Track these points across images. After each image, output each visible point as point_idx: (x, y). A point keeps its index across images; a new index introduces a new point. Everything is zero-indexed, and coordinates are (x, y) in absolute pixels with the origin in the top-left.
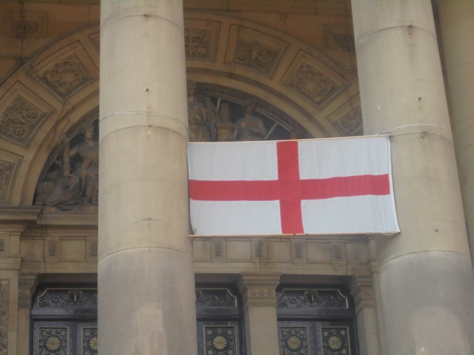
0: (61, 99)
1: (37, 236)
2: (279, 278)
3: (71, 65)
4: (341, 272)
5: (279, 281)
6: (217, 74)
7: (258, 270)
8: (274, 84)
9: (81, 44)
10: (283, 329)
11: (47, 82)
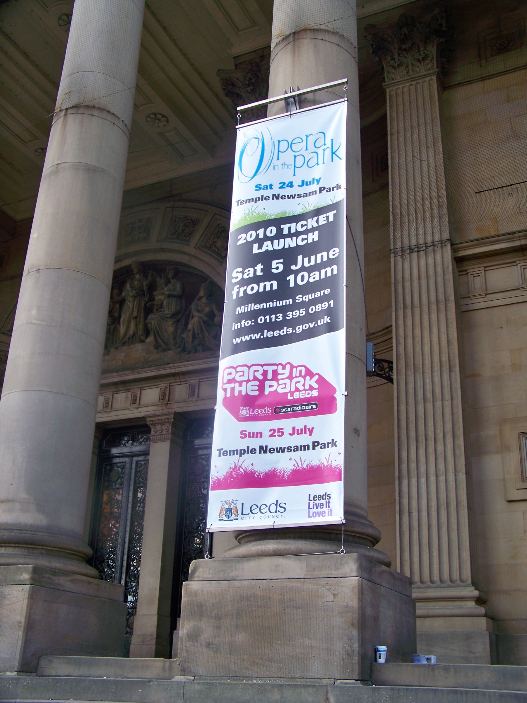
2: (172, 416)
7: (161, 411)
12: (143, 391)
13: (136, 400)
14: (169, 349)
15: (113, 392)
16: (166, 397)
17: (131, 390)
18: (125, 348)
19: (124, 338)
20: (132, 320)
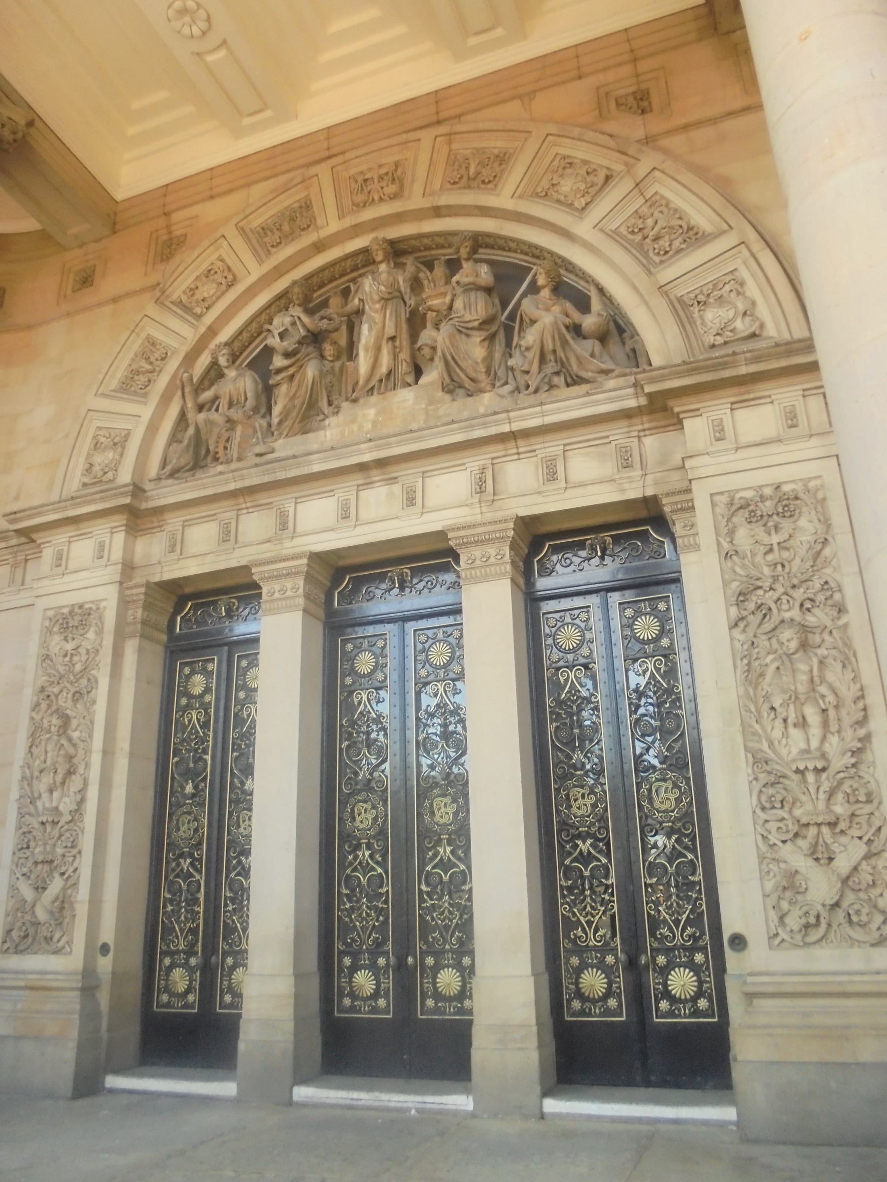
1: (154, 528)
2: (512, 525)
4: (633, 493)
5: (514, 529)
7: (479, 516)
8: (502, 199)
10: (549, 616)
12: (427, 480)
13: (414, 499)
14: (482, 391)
15: (358, 486)
16: (485, 488)
17: (399, 479)
18: (374, 399)
19: (368, 380)
20: (384, 342)
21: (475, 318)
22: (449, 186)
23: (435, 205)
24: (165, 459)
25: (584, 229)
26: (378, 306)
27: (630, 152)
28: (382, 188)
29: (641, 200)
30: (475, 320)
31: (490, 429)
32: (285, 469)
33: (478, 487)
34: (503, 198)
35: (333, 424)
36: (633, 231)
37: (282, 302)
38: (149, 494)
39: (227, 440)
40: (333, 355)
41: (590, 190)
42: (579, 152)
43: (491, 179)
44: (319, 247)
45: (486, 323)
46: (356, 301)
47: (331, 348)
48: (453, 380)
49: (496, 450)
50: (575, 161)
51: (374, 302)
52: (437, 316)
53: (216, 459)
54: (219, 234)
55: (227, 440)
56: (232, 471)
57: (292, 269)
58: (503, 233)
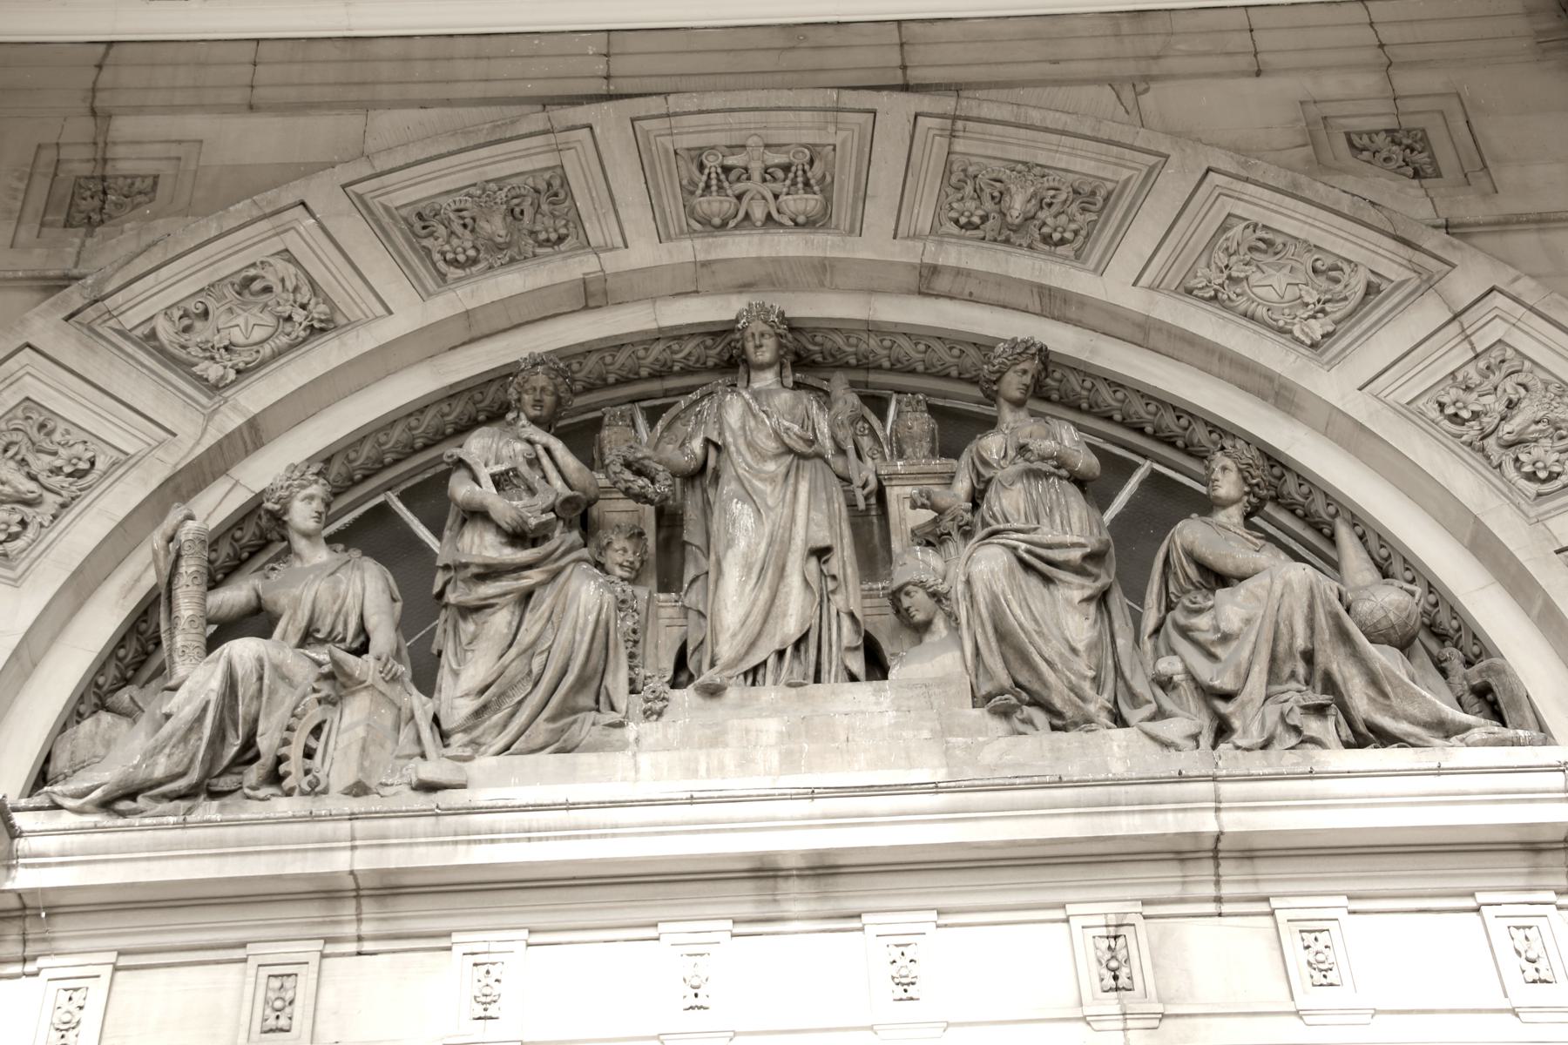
0: (204, 400)
3: (267, 290)
6: (875, 280)
8: (1114, 284)
9: (313, 215)
11: (162, 353)
18: (769, 693)
19: (753, 645)
21: (1069, 539)
22: (955, 230)
23: (927, 260)
24: (48, 760)
25: (1331, 385)
26: (771, 466)
27: (1426, 246)
28: (776, 197)
29: (1462, 354)
30: (1074, 545)
31: (1160, 817)
32: (529, 835)
33: (1108, 975)
34: (1114, 284)
35: (648, 741)
36: (1456, 415)
37: (485, 403)
38: (22, 844)
39: (317, 731)
40: (631, 566)
41: (1328, 307)
42: (1292, 220)
43: (1068, 235)
44: (591, 296)
45: (1095, 557)
46: (697, 445)
47: (627, 544)
48: (1017, 684)
49: (1163, 881)
50: (1279, 240)
51: (763, 457)
52: (935, 520)
53: (275, 778)
54: (288, 196)
55: (317, 731)
56: (353, 817)
57: (505, 330)
58: (1098, 361)
